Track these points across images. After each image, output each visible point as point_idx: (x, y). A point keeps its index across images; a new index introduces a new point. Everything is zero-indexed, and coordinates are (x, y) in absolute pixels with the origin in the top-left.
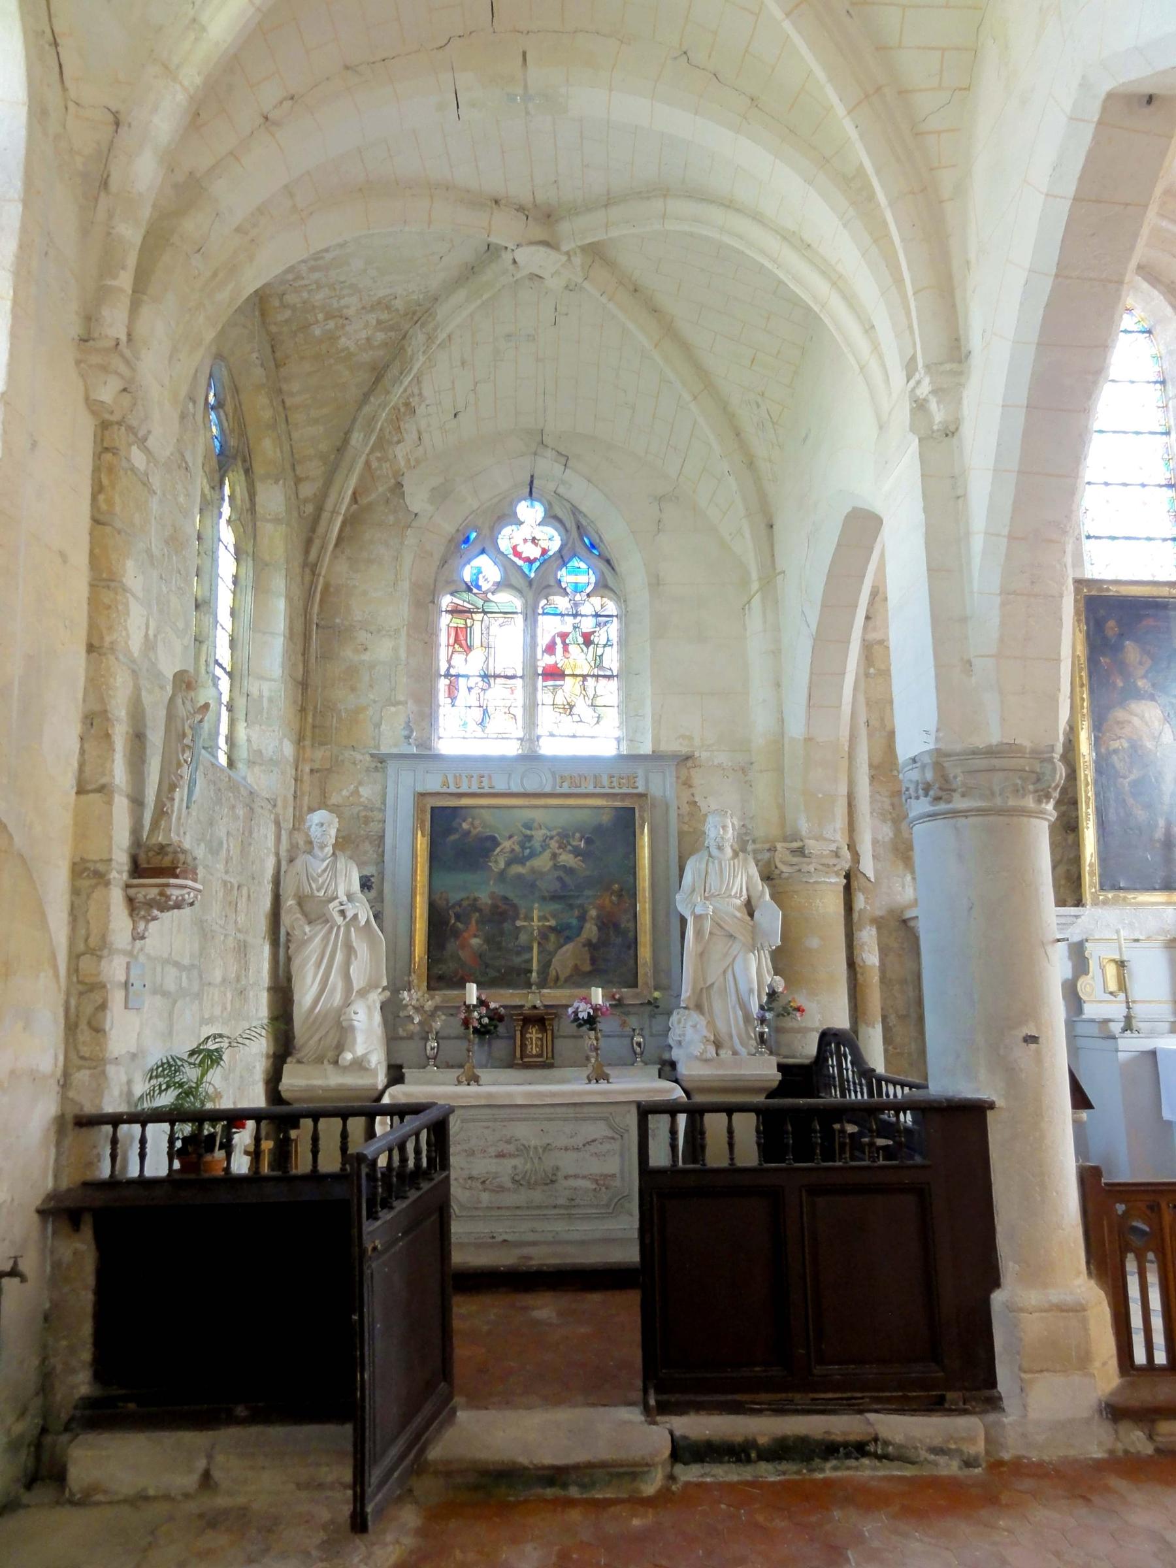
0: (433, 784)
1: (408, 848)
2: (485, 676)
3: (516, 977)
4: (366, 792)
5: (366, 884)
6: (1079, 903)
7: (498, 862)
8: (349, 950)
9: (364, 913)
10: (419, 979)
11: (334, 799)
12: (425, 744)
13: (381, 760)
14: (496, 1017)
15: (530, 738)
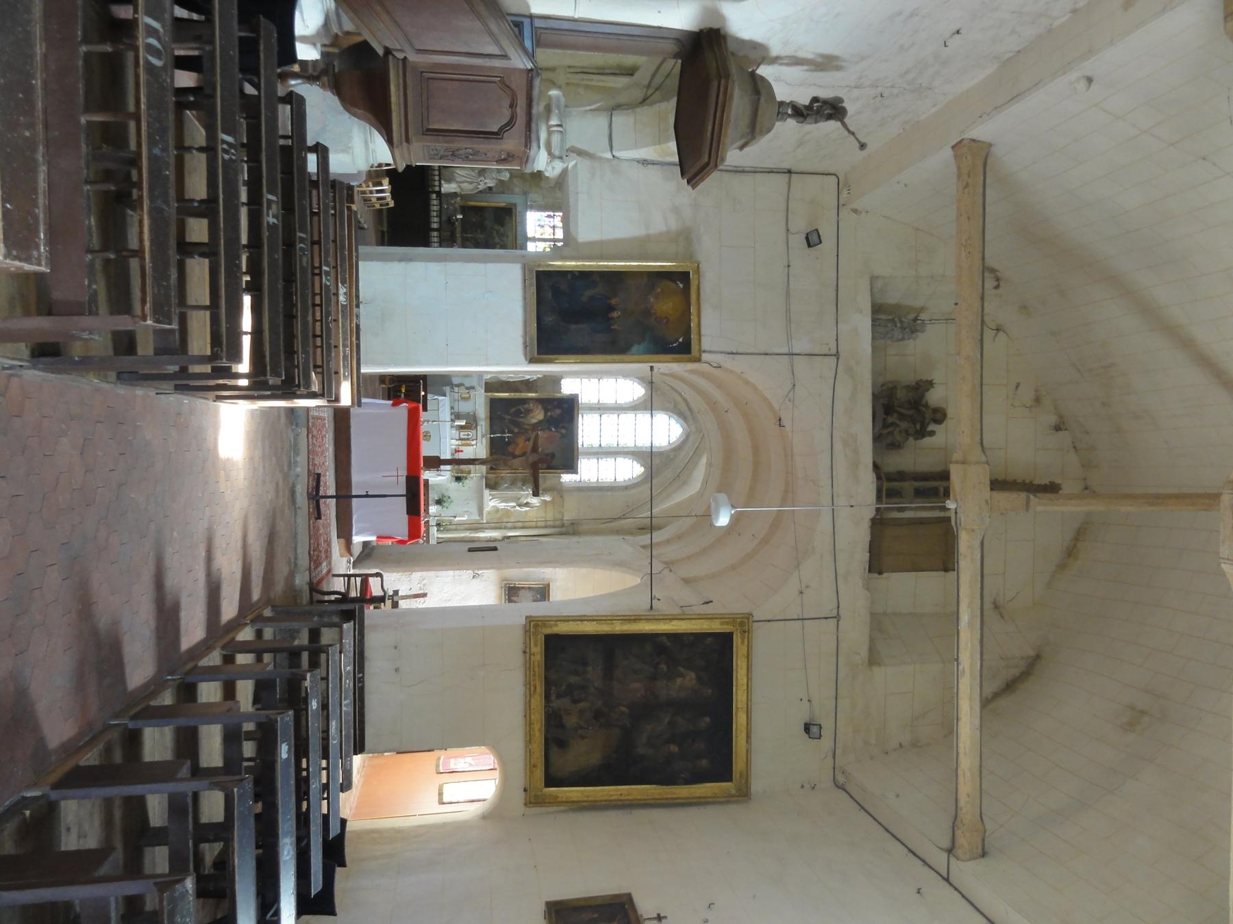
0: (519, 209)
1: (501, 201)
2: (554, 227)
3: (464, 230)
4: (517, 190)
5: (490, 188)
6: (486, 391)
7: (496, 227)
8: (471, 183)
9: (481, 187)
10: (462, 203)
11: (515, 180)
12: (532, 208)
13: (525, 194)
14: (453, 224)
15: (534, 239)
